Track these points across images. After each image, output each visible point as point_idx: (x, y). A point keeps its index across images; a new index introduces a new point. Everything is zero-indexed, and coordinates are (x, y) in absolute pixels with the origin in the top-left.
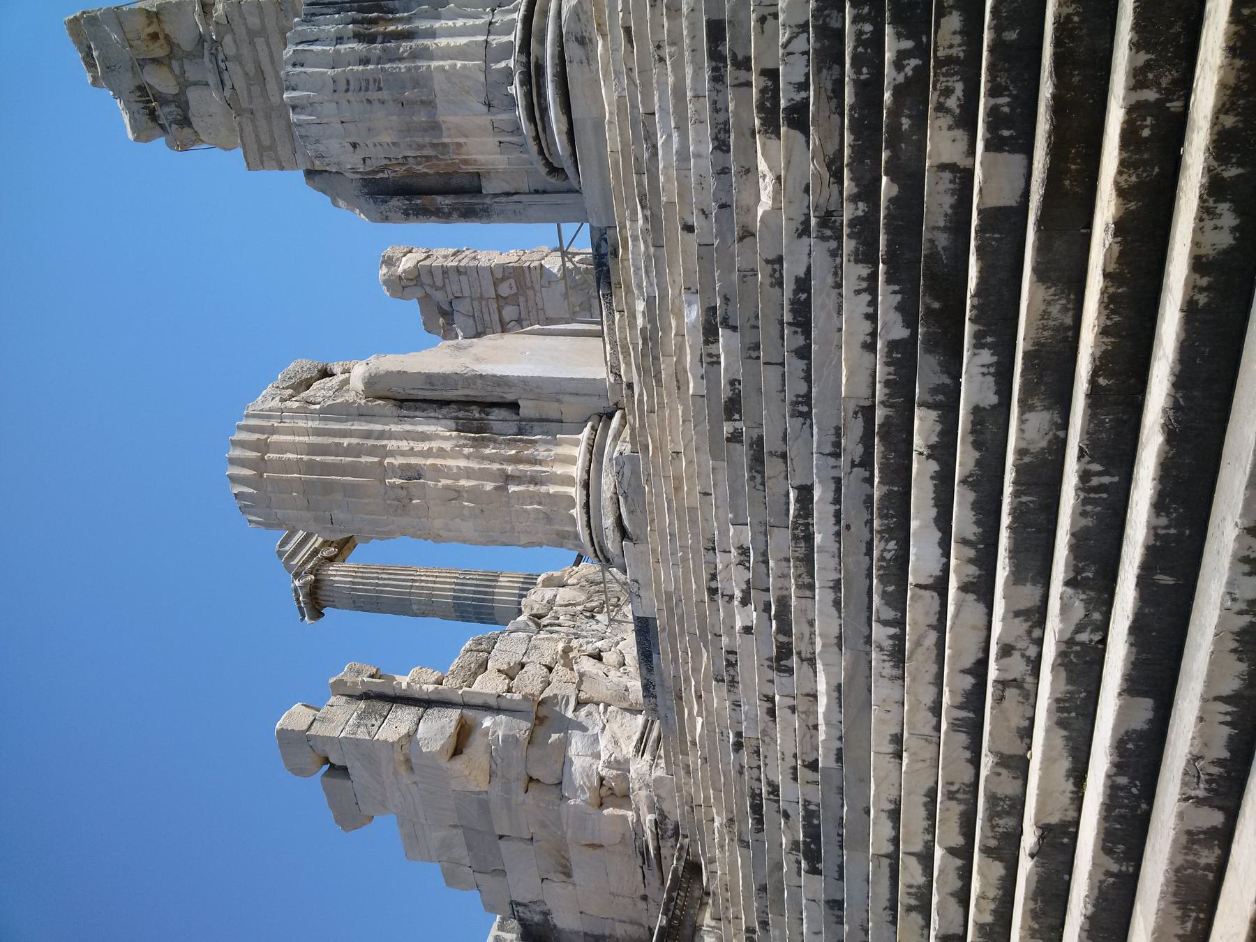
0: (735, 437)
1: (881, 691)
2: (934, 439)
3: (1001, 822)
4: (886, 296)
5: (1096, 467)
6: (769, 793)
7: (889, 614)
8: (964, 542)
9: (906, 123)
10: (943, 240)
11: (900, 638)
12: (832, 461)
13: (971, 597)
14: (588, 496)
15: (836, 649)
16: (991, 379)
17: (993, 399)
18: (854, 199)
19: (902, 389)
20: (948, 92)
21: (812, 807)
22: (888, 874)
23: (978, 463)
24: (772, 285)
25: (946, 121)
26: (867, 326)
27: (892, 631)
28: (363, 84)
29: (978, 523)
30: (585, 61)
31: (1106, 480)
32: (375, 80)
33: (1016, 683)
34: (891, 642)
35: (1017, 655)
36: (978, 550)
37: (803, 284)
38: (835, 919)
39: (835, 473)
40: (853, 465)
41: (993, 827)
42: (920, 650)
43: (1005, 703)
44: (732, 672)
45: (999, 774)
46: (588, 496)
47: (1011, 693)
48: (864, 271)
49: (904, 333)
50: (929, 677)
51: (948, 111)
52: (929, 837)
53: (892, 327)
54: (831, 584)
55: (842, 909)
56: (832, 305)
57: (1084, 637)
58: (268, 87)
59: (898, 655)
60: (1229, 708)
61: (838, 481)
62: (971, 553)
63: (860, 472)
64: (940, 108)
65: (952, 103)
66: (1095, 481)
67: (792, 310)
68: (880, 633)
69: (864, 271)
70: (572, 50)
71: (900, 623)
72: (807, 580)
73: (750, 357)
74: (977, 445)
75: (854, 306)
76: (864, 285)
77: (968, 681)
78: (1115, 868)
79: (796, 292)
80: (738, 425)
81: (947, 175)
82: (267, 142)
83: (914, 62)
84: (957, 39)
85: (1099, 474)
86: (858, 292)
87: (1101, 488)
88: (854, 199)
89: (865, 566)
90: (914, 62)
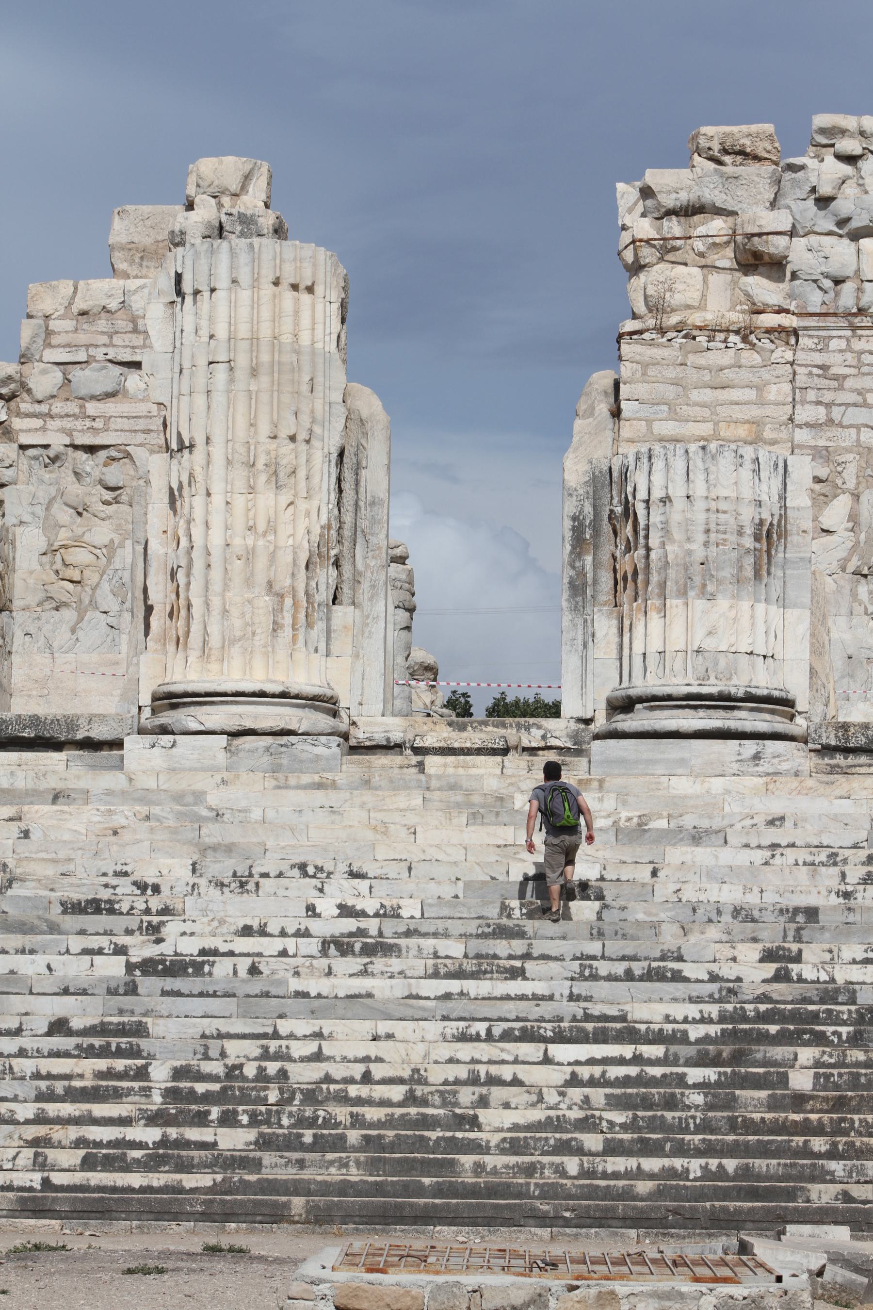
0: (505, 909)
1: (433, 1029)
2: (646, 1056)
3: (436, 1097)
4: (713, 1030)
5: (698, 1121)
6: (149, 923)
7: (497, 1031)
8: (604, 1073)
9: (806, 1037)
10: (759, 1056)
11: (477, 1038)
12: (566, 992)
13: (568, 1077)
14: (273, 696)
15: (406, 994)
16: (702, 1080)
17: (690, 1082)
18: (756, 1010)
19: (658, 1038)
20: (831, 1056)
21: (207, 968)
22: (255, 1032)
23: (654, 1077)
24: (662, 950)
25: (817, 1055)
26: (680, 1018)
27: (483, 1034)
28: (722, 528)
29: (617, 1078)
30: (740, 758)
31: (692, 1126)
32: (725, 540)
33: (541, 1099)
34: (474, 1033)
35: (561, 1098)
36: (599, 1079)
37: (678, 977)
38: (113, 985)
39: (557, 996)
40: (584, 1009)
41: (431, 1093)
42: (498, 1051)
43: (527, 1095)
44: (233, 885)
45: (474, 1094)
46: (273, 696)
47: (534, 1098)
48: (715, 1015)
49: (692, 1038)
50: (477, 1056)
51: (822, 1056)
52: (338, 1059)
53: (695, 1032)
54: (465, 991)
55: (126, 994)
56: (677, 994)
57: (604, 1124)
58: (708, 391)
59: (463, 1038)
60: (635, 1168)
61: (551, 998)
62: (597, 1075)
63: (580, 1013)
64: (824, 1052)
65: (826, 1058)
66: (691, 1121)
67: (659, 967)
68: (481, 1028)
69: (715, 1015)
70: (750, 747)
71: (490, 1037)
72: (442, 971)
73: (592, 928)
74: (664, 1076)
75: (693, 1011)
76: (706, 1016)
77: (508, 1077)
78: (492, 1144)
79: (672, 970)
80: (517, 913)
81: (792, 1057)
82: (652, 372)
83: (836, 1040)
84: (854, 1059)
85: (695, 1123)
86: (701, 1012)
87: (688, 1124)
88: (756, 1010)
89: (508, 1016)
90: (836, 1040)
